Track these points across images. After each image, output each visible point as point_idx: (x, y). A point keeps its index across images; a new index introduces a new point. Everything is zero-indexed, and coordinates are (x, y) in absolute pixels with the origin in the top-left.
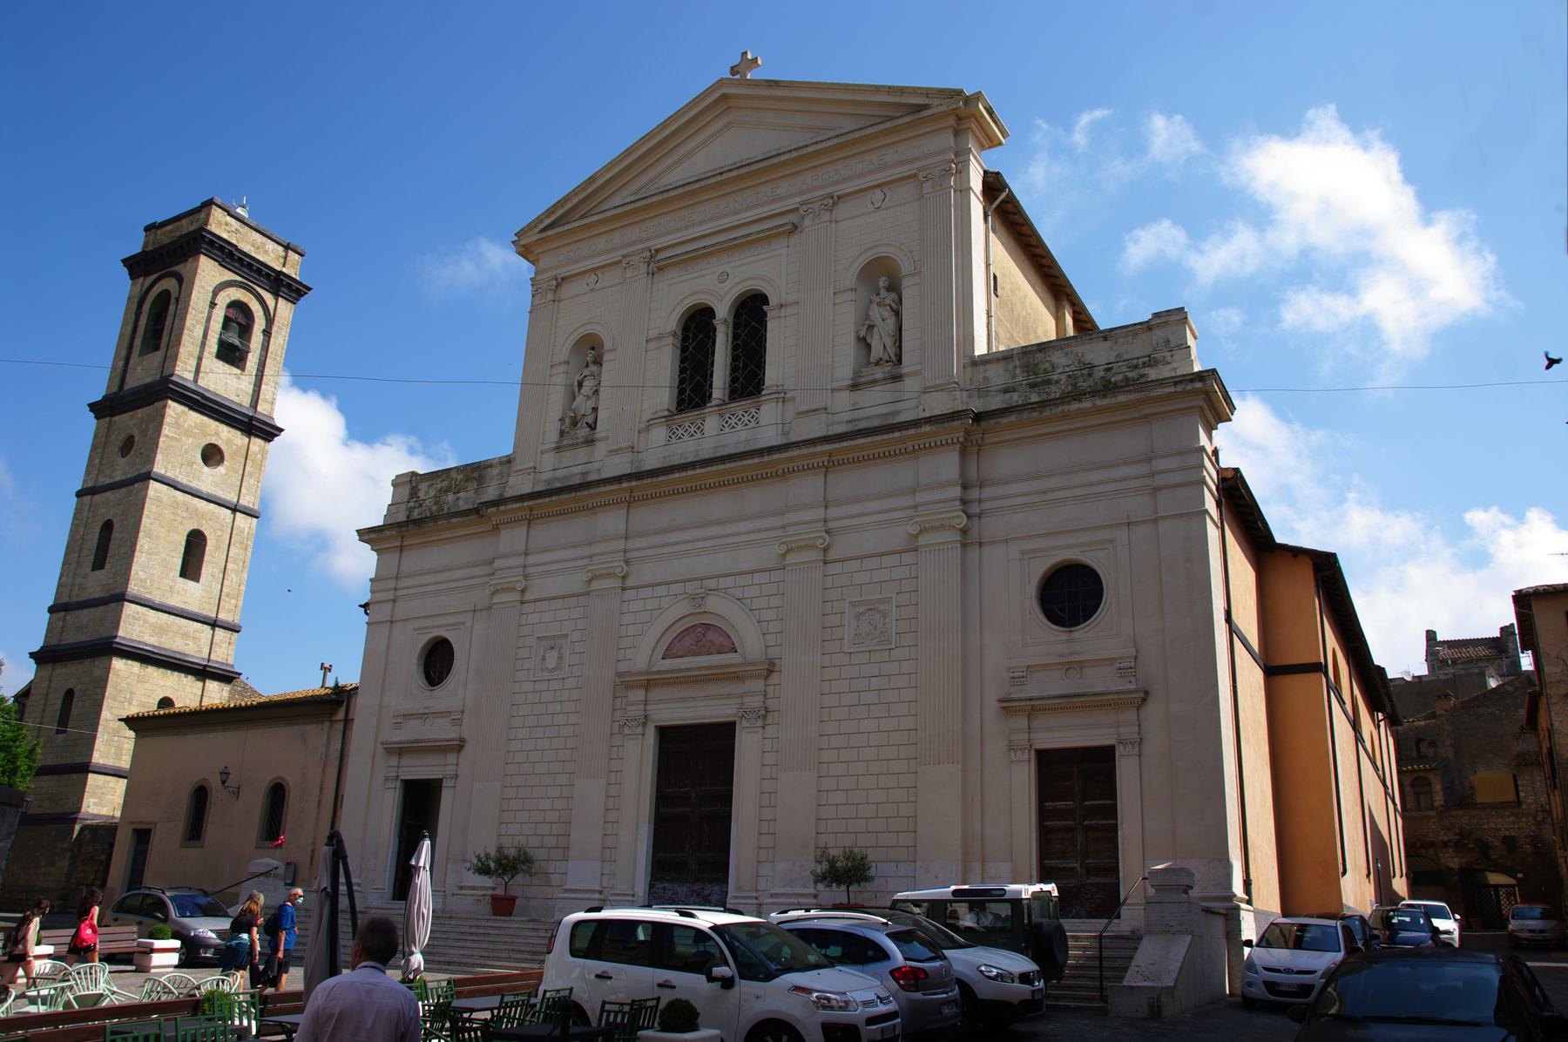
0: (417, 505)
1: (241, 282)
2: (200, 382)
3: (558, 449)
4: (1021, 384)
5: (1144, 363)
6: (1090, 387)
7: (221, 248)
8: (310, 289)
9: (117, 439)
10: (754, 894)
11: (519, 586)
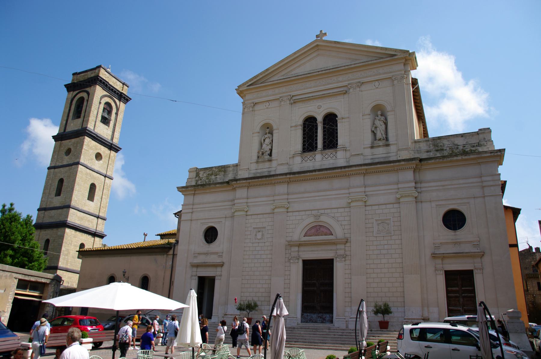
0: (199, 179)
1: (109, 96)
2: (96, 131)
3: (257, 162)
4: (433, 150)
5: (477, 145)
6: (458, 152)
7: (104, 83)
8: (131, 99)
9: (64, 149)
10: (344, 318)
11: (246, 210)
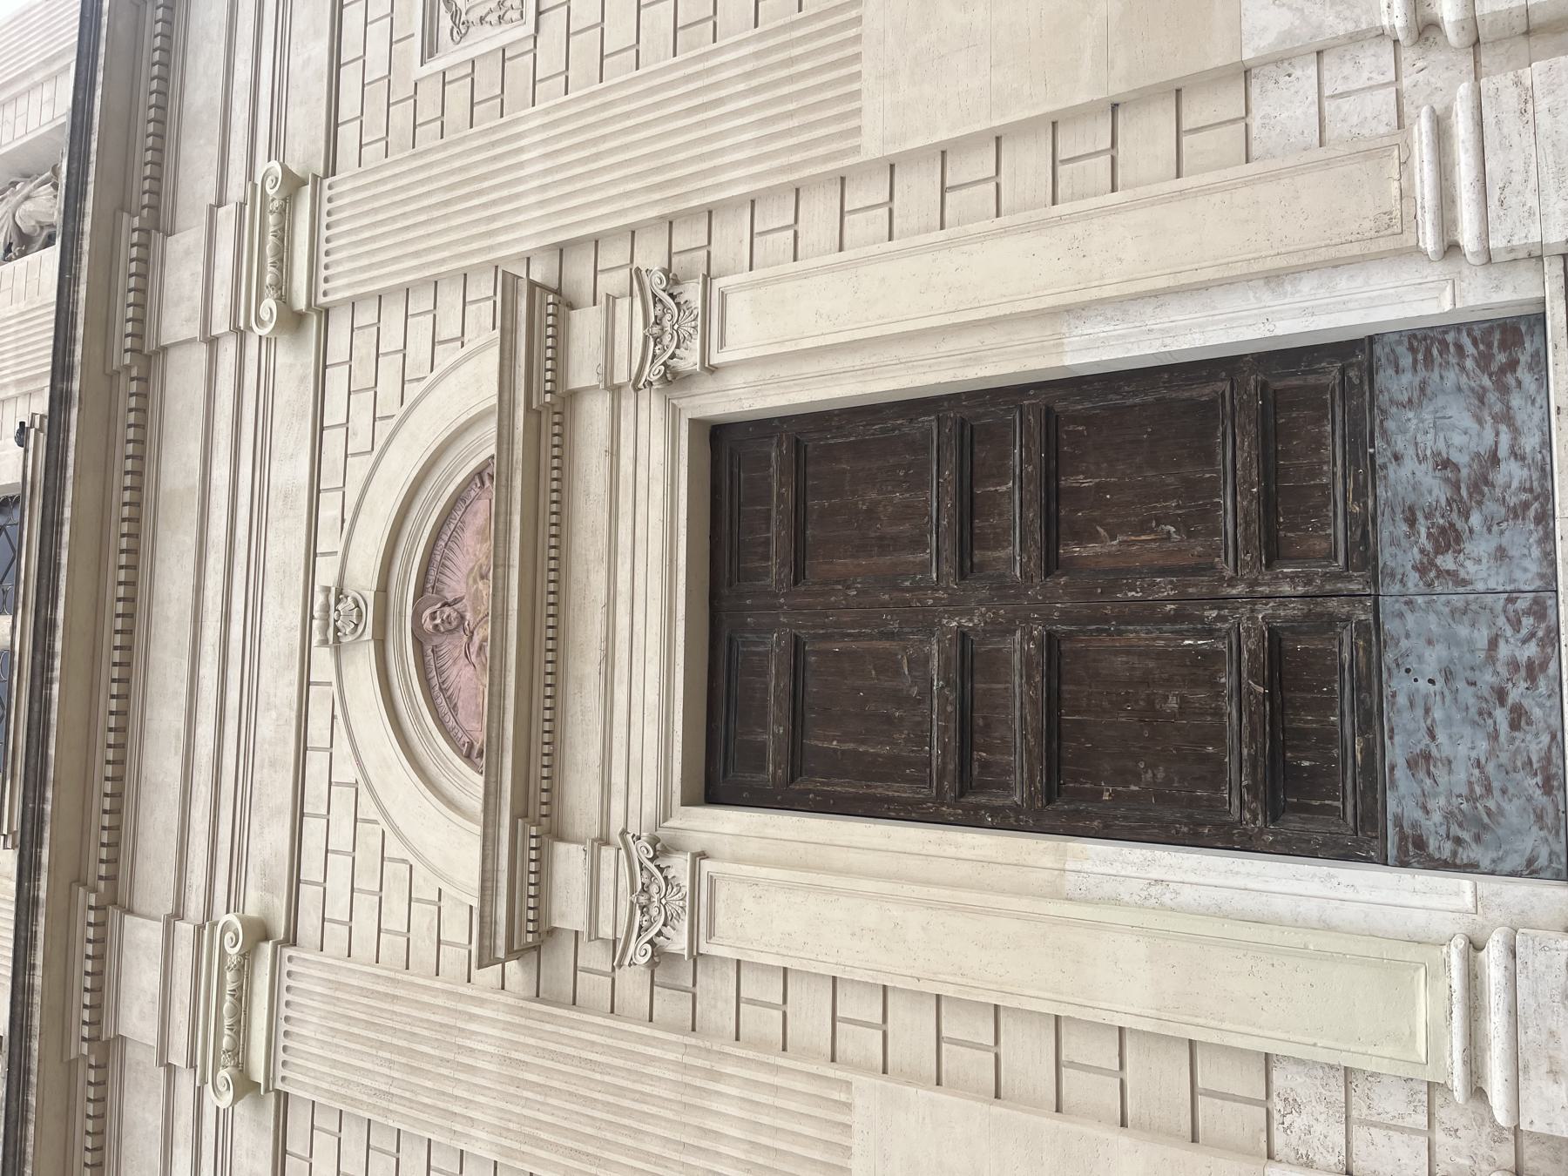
10: (1422, 130)
